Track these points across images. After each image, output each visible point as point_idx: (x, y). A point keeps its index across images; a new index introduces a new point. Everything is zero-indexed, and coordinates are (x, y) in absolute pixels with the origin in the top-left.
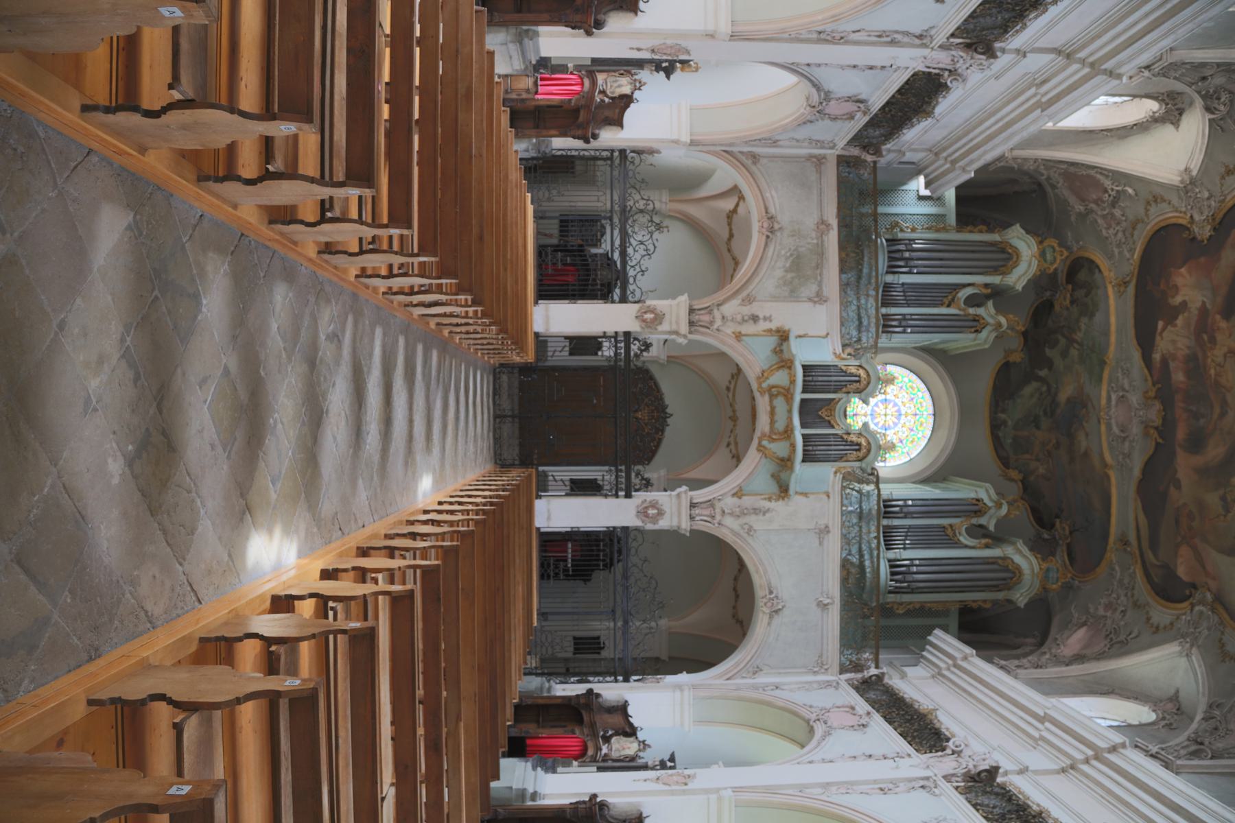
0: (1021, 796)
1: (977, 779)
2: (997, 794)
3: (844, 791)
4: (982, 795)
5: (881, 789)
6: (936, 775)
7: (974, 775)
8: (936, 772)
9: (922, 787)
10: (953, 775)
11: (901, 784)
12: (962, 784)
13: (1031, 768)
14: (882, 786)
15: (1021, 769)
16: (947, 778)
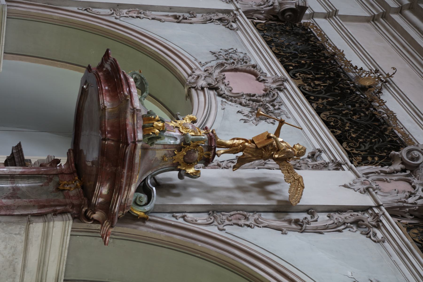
0: (320, 38)
1: (280, 18)
2: (296, 34)
3: (135, 15)
4: (281, 34)
5: (176, 17)
6: (237, 9)
7: (278, 13)
8: (238, 6)
9: (220, 20)
10: (256, 11)
11: (199, 16)
12: (264, 22)
13: (340, 13)
14: (178, 14)
15: (329, 13)
16: (249, 13)
